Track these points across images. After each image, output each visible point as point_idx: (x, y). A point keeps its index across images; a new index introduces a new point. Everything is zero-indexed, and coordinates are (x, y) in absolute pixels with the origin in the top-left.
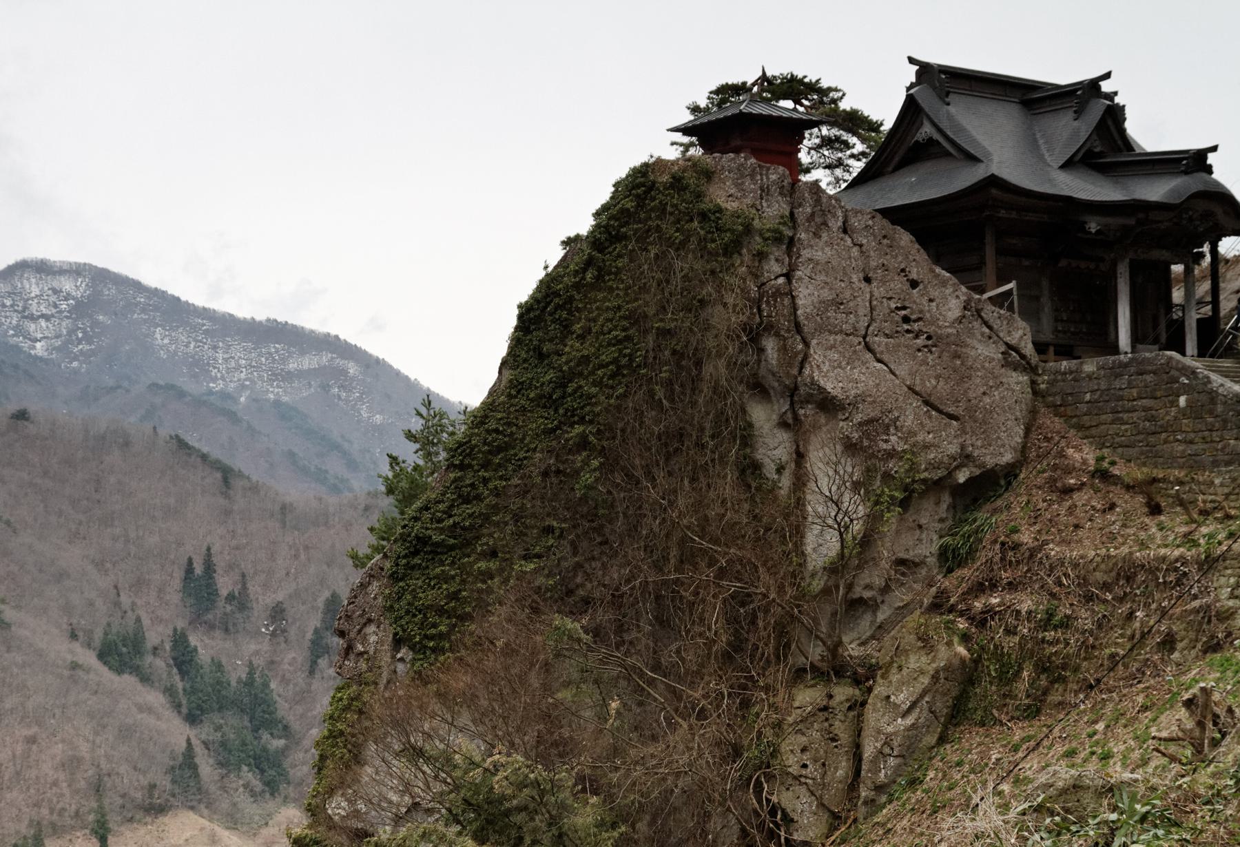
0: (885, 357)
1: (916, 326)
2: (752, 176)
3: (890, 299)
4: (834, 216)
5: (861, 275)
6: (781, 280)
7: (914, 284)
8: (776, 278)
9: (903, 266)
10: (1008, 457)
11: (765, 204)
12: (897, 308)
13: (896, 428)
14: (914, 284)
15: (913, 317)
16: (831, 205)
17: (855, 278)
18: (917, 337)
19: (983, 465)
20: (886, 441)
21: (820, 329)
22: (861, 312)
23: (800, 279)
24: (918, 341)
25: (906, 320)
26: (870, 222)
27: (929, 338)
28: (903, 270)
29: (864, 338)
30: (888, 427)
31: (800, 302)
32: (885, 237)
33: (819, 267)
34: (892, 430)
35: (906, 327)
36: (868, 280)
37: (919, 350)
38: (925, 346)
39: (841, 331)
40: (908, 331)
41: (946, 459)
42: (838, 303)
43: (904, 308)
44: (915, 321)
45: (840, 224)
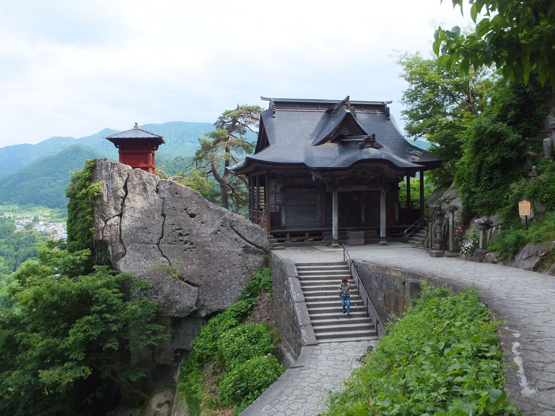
0: (166, 254)
1: (186, 238)
3: (173, 224)
6: (116, 218)
7: (192, 216)
8: (114, 217)
9: (186, 207)
12: (176, 229)
13: (162, 292)
14: (192, 216)
15: (184, 234)
17: (156, 216)
18: (186, 243)
20: (156, 298)
21: (132, 242)
25: (180, 235)
27: (192, 244)
28: (186, 209)
29: (158, 244)
30: (157, 291)
32: (177, 193)
34: (160, 293)
35: (180, 238)
36: (164, 215)
37: (185, 250)
38: (189, 248)
39: (144, 242)
40: (181, 240)
43: (181, 229)
44: (185, 235)
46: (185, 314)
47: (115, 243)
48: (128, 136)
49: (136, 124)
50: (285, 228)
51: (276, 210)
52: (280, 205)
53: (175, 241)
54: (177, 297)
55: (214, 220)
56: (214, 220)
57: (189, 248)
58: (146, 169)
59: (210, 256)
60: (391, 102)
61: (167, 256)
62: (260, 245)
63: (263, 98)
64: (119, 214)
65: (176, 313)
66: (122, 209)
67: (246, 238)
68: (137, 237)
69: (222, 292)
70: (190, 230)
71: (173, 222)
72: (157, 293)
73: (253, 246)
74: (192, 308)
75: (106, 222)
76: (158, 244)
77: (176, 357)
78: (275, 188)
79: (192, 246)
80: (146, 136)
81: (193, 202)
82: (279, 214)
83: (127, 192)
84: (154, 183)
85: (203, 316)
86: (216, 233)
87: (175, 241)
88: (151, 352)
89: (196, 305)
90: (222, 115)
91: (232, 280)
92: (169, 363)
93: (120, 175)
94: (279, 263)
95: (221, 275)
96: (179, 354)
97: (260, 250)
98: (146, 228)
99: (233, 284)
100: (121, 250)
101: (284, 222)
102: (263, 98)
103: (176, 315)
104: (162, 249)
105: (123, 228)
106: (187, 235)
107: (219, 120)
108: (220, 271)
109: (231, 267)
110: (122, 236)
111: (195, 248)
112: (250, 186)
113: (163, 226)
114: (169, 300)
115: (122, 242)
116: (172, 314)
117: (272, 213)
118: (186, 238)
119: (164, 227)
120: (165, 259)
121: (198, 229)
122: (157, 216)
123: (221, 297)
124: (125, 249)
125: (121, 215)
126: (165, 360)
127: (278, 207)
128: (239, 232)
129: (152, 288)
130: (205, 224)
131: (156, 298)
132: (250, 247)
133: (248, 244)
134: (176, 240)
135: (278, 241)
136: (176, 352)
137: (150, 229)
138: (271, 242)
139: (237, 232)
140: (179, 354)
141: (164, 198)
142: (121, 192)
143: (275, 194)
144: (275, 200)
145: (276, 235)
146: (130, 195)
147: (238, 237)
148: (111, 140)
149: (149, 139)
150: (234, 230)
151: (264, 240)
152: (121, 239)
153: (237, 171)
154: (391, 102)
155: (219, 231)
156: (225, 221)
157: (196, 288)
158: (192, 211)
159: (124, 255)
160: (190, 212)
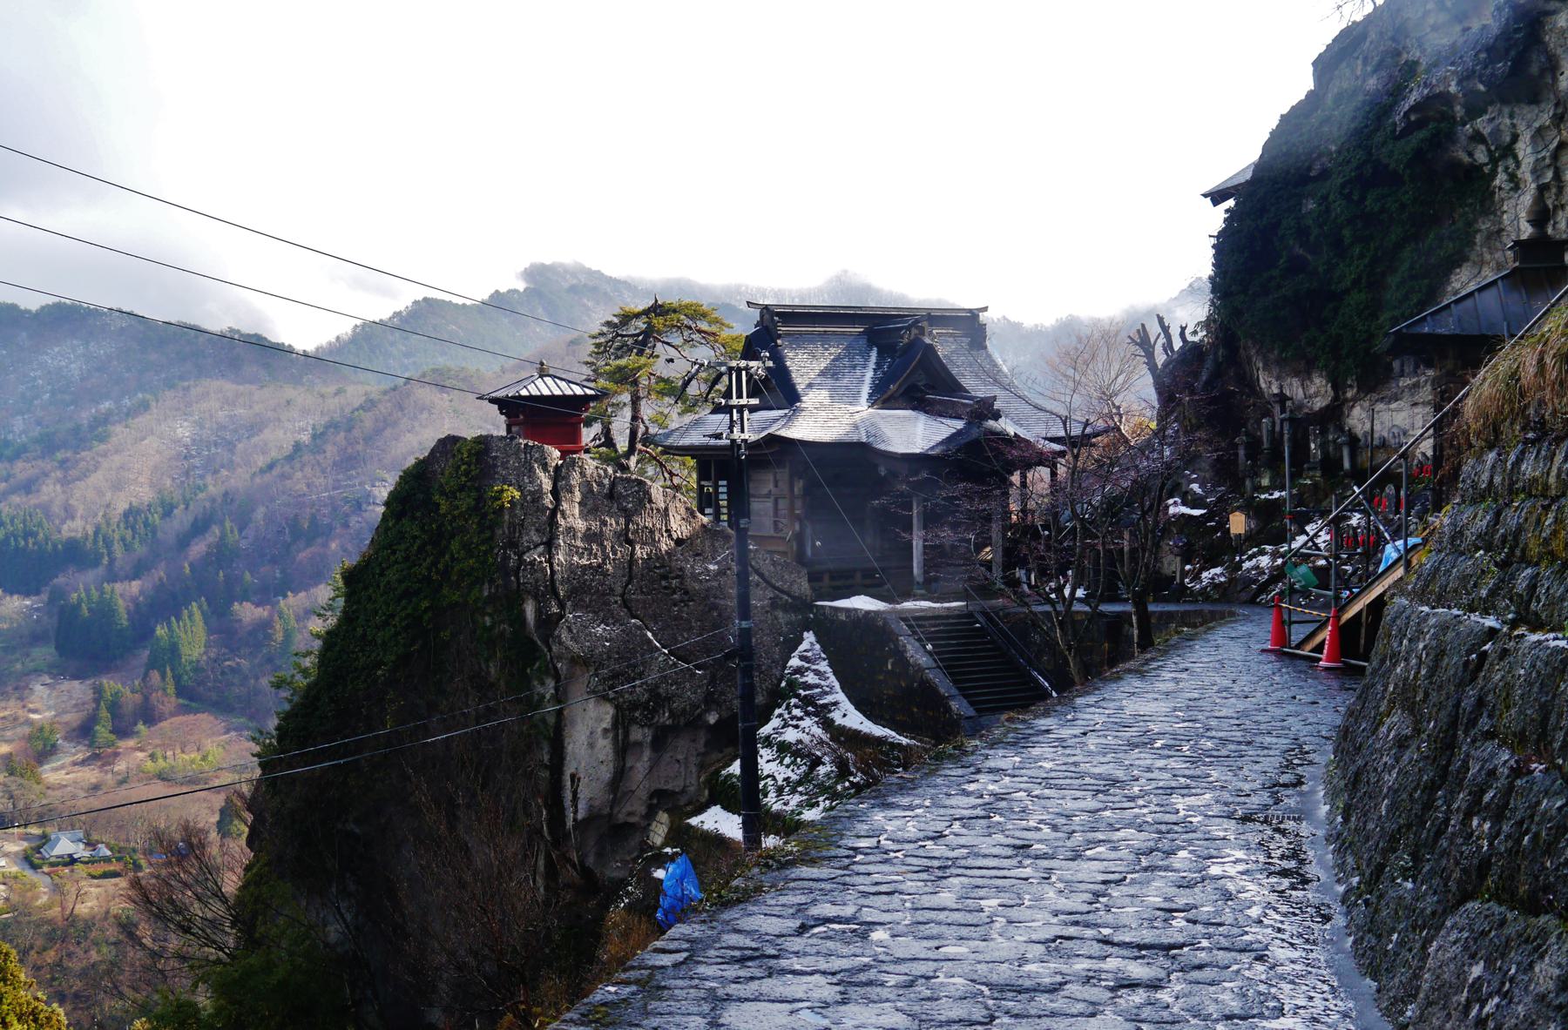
6: (541, 549)
8: (536, 546)
25: (664, 577)
29: (622, 596)
47: (544, 595)
56: (715, 552)
59: (720, 615)
60: (985, 309)
70: (681, 569)
75: (521, 555)
84: (606, 481)
90: (616, 320)
93: (545, 467)
100: (555, 610)
105: (557, 568)
107: (605, 329)
126: (630, 814)
142: (548, 500)
146: (565, 506)
151: (803, 586)
154: (985, 309)
159: (561, 616)
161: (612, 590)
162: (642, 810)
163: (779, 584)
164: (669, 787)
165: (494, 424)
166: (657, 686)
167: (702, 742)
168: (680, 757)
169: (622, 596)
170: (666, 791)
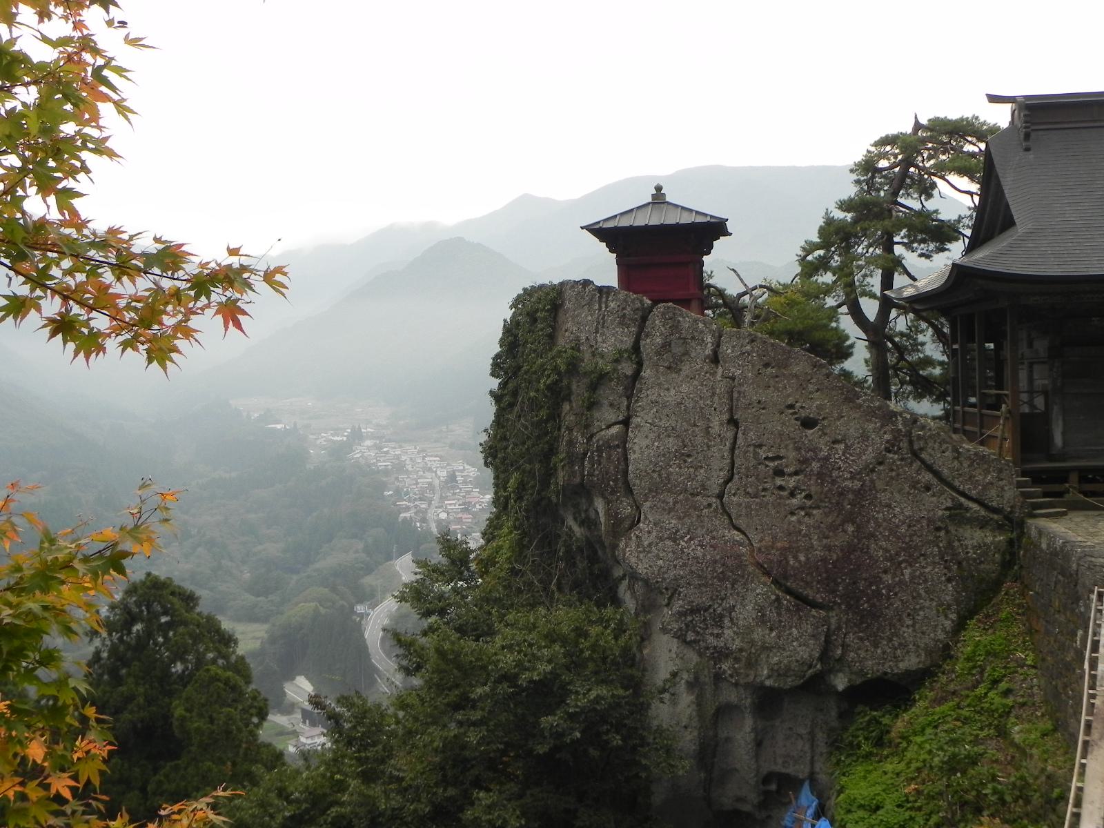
0: (742, 523)
1: (792, 482)
2: (590, 304)
3: (760, 446)
4: (702, 342)
5: (725, 417)
6: (615, 430)
7: (808, 423)
8: (608, 427)
9: (790, 401)
10: (911, 662)
11: (600, 339)
12: (766, 458)
13: (732, 620)
14: (808, 423)
16: (696, 329)
18: (792, 495)
19: (861, 672)
20: (718, 636)
21: (654, 490)
22: (716, 464)
23: (638, 426)
24: (794, 501)
25: (779, 473)
26: (748, 348)
27: (808, 497)
28: (791, 406)
30: (721, 616)
31: (632, 457)
32: (767, 365)
33: (666, 411)
34: (727, 622)
35: (779, 481)
37: (792, 514)
40: (781, 488)
41: (794, 665)
42: (682, 456)
43: (778, 458)
44: (791, 475)
45: (708, 352)
46: (790, 682)
48: (641, 220)
49: (659, 188)
50: (1062, 457)
51: (1032, 406)
52: (1045, 393)
53: (764, 490)
54: (774, 634)
55: (864, 437)
57: (802, 508)
58: (685, 302)
59: (859, 528)
61: (743, 527)
62: (994, 504)
63: (993, 99)
64: (621, 418)
65: (769, 677)
66: (628, 407)
67: (957, 483)
68: (668, 478)
69: (891, 625)
71: (759, 437)
72: (718, 621)
73: (975, 507)
74: (810, 667)
76: (720, 496)
77: (767, 794)
78: (1030, 345)
79: (808, 503)
80: (686, 219)
81: (810, 386)
82: (1045, 418)
83: (640, 364)
85: (841, 687)
86: (873, 471)
87: (764, 490)
88: (702, 775)
89: (821, 659)
91: (919, 595)
92: (746, 808)
94: (1055, 554)
95: (888, 579)
96: (773, 787)
97: (996, 517)
98: (689, 456)
99: (922, 608)
101: (1058, 440)
102: (993, 99)
103: (768, 683)
104: (733, 511)
106: (796, 473)
108: (885, 572)
109: (916, 561)
110: (631, 476)
111: (818, 507)
112: (955, 342)
113: (733, 449)
114: (752, 643)
115: (629, 491)
116: (758, 680)
117: (1023, 415)
118: (792, 482)
119: (737, 452)
120: (738, 537)
121: (827, 459)
122: (717, 423)
123: (890, 640)
124: (638, 508)
125: (626, 423)
126: (740, 799)
127: (1040, 402)
128: (936, 467)
129: (706, 610)
130: (842, 446)
131: (718, 636)
132: (967, 509)
133: (963, 500)
134: (768, 486)
135: (1045, 495)
136: (767, 779)
137: (700, 457)
138: (1026, 495)
139: (929, 468)
140: (773, 787)
141: (733, 378)
143: (1031, 365)
144: (1031, 380)
145: (1037, 478)
146: (647, 373)
147: (935, 481)
148: (599, 232)
149: (693, 226)
150: (923, 461)
152: (626, 483)
153: (922, 305)
155: (880, 463)
156: (895, 438)
157: (823, 613)
158: (810, 411)
159: (635, 522)
160: (803, 414)
161: (704, 487)
162: (754, 798)
163: (966, 487)
164: (790, 770)
165: (602, 267)
166: (749, 630)
167: (834, 713)
168: (803, 731)
169: (720, 496)
170: (788, 775)
